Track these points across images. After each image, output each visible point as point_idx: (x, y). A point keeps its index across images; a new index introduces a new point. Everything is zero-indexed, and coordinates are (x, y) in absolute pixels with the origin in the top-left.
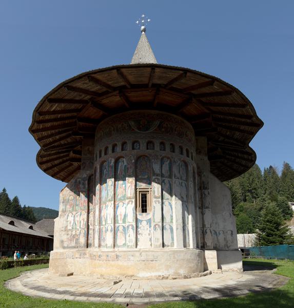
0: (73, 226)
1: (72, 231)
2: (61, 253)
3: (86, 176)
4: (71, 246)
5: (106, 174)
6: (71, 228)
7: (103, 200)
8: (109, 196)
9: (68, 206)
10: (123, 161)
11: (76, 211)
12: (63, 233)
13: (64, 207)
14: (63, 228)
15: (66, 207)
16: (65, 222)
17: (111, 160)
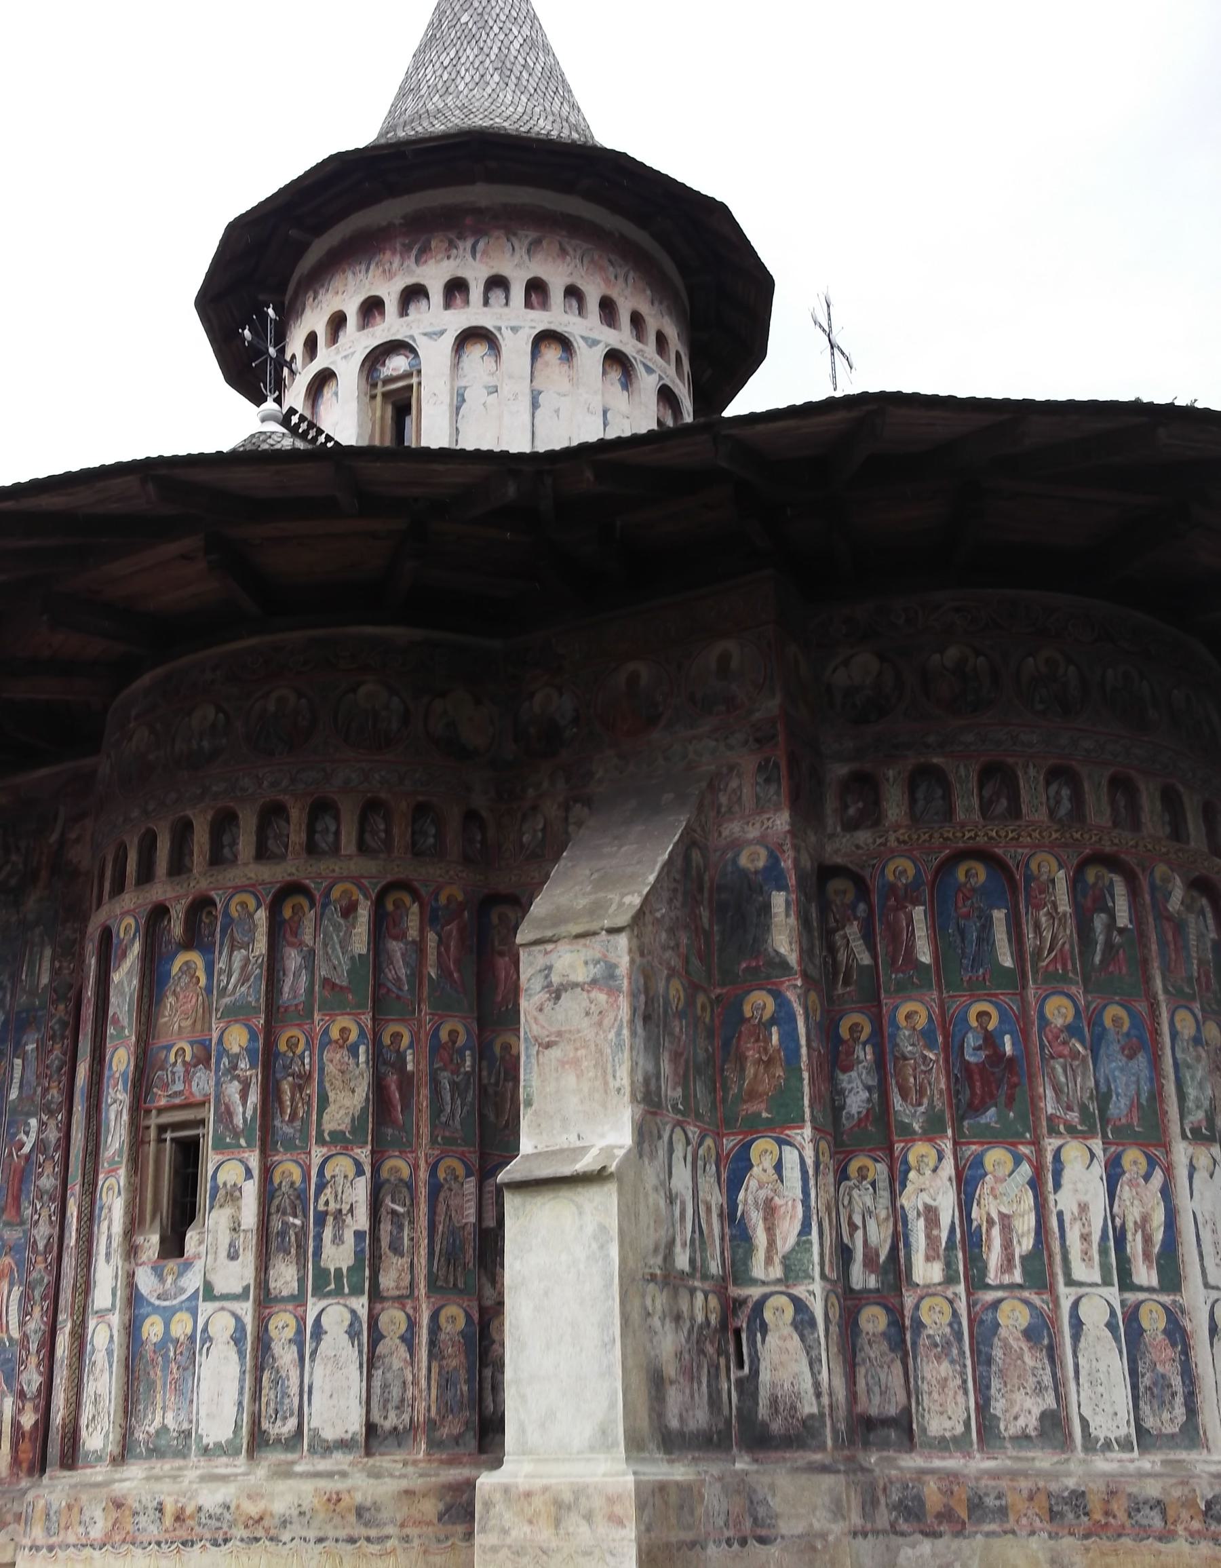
0: (692, 1240)
1: (692, 1291)
2: (677, 1484)
3: (809, 865)
4: (692, 1426)
5: (1109, 944)
6: (687, 1268)
7: (1119, 1107)
8: (1190, 1104)
9: (666, 1067)
10: (1202, 912)
11: (698, 1116)
12: (658, 1300)
13: (650, 1067)
14: (656, 1250)
15: (657, 1065)
16: (662, 1203)
17: (1166, 880)
